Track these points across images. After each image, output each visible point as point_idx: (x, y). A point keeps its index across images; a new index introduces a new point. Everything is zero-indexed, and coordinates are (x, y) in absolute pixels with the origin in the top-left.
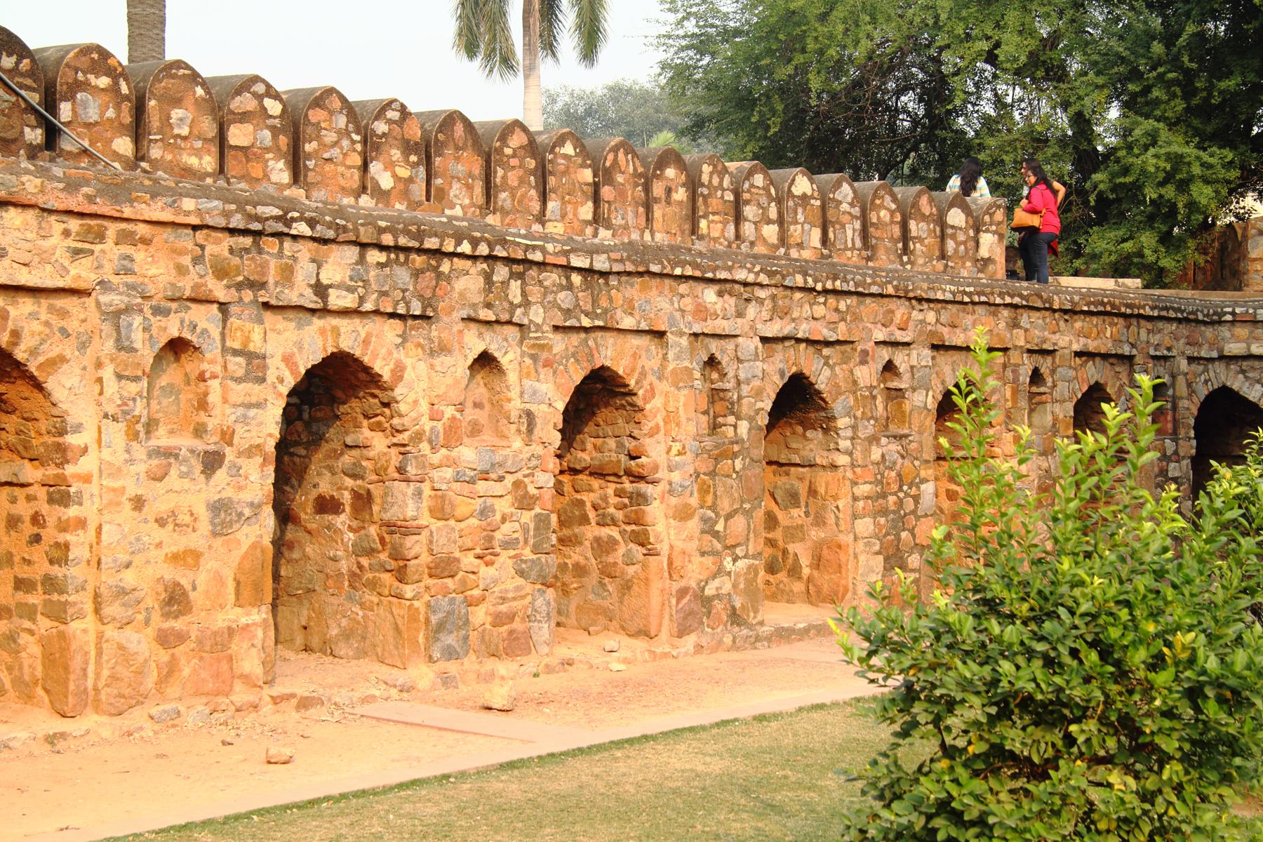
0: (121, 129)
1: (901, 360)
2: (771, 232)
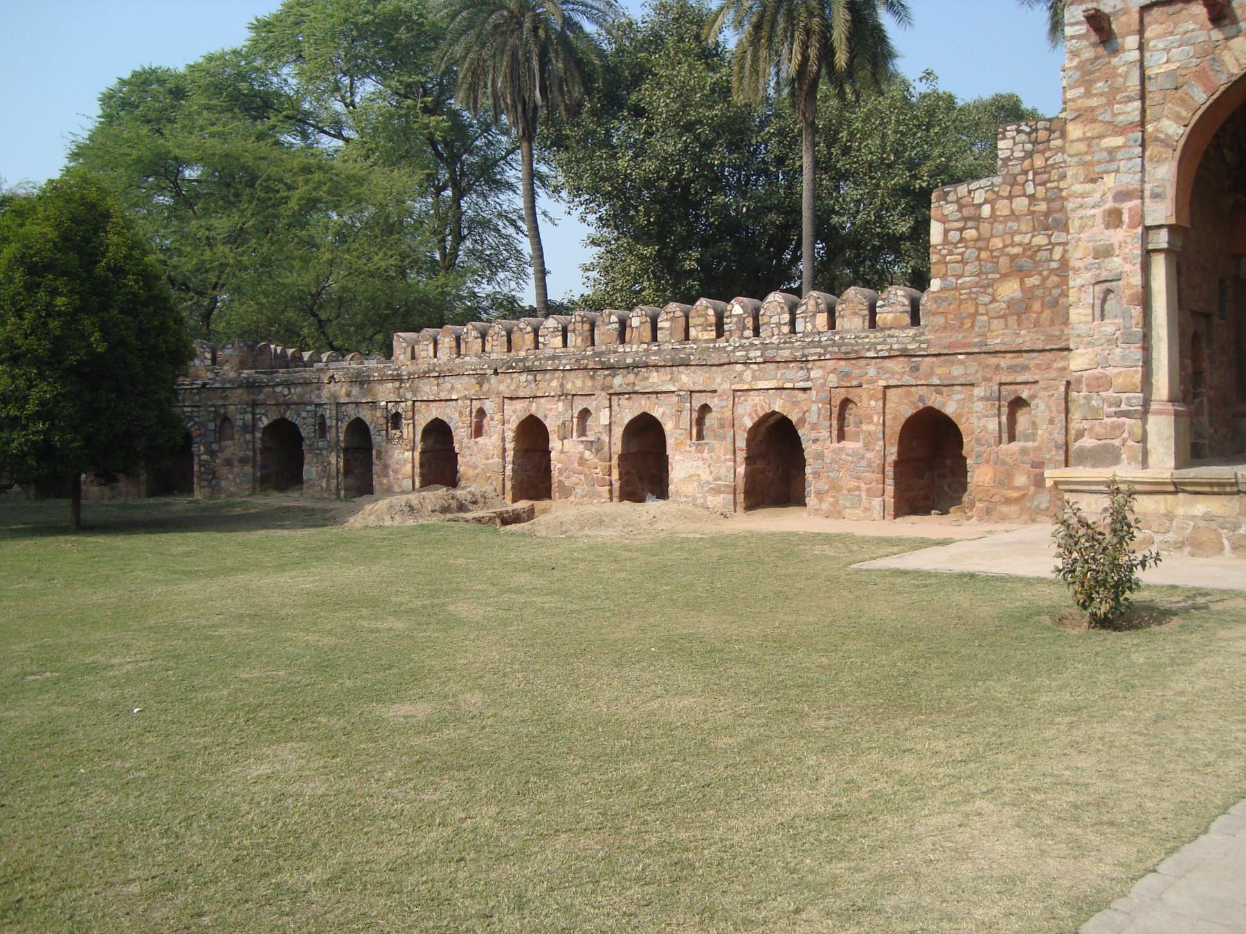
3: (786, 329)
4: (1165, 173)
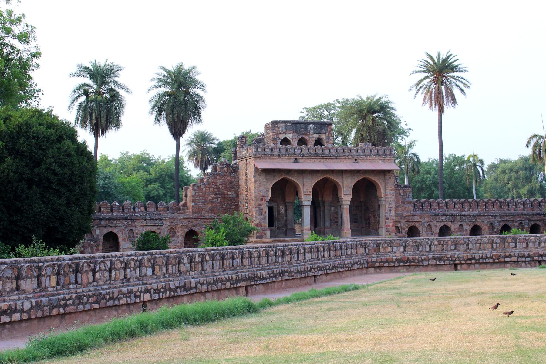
1: (523, 222)
2: (514, 207)
3: (132, 210)
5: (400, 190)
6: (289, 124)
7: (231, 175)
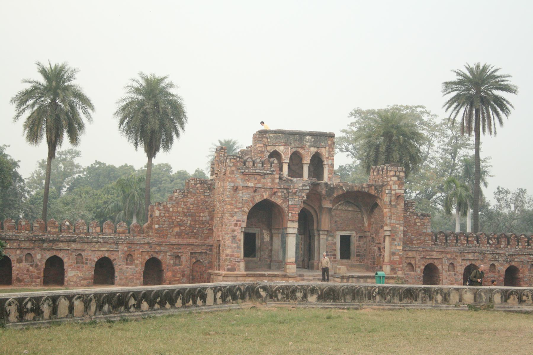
0: (455, 240)
4: (245, 217)
5: (416, 219)
6: (280, 135)
7: (206, 194)
